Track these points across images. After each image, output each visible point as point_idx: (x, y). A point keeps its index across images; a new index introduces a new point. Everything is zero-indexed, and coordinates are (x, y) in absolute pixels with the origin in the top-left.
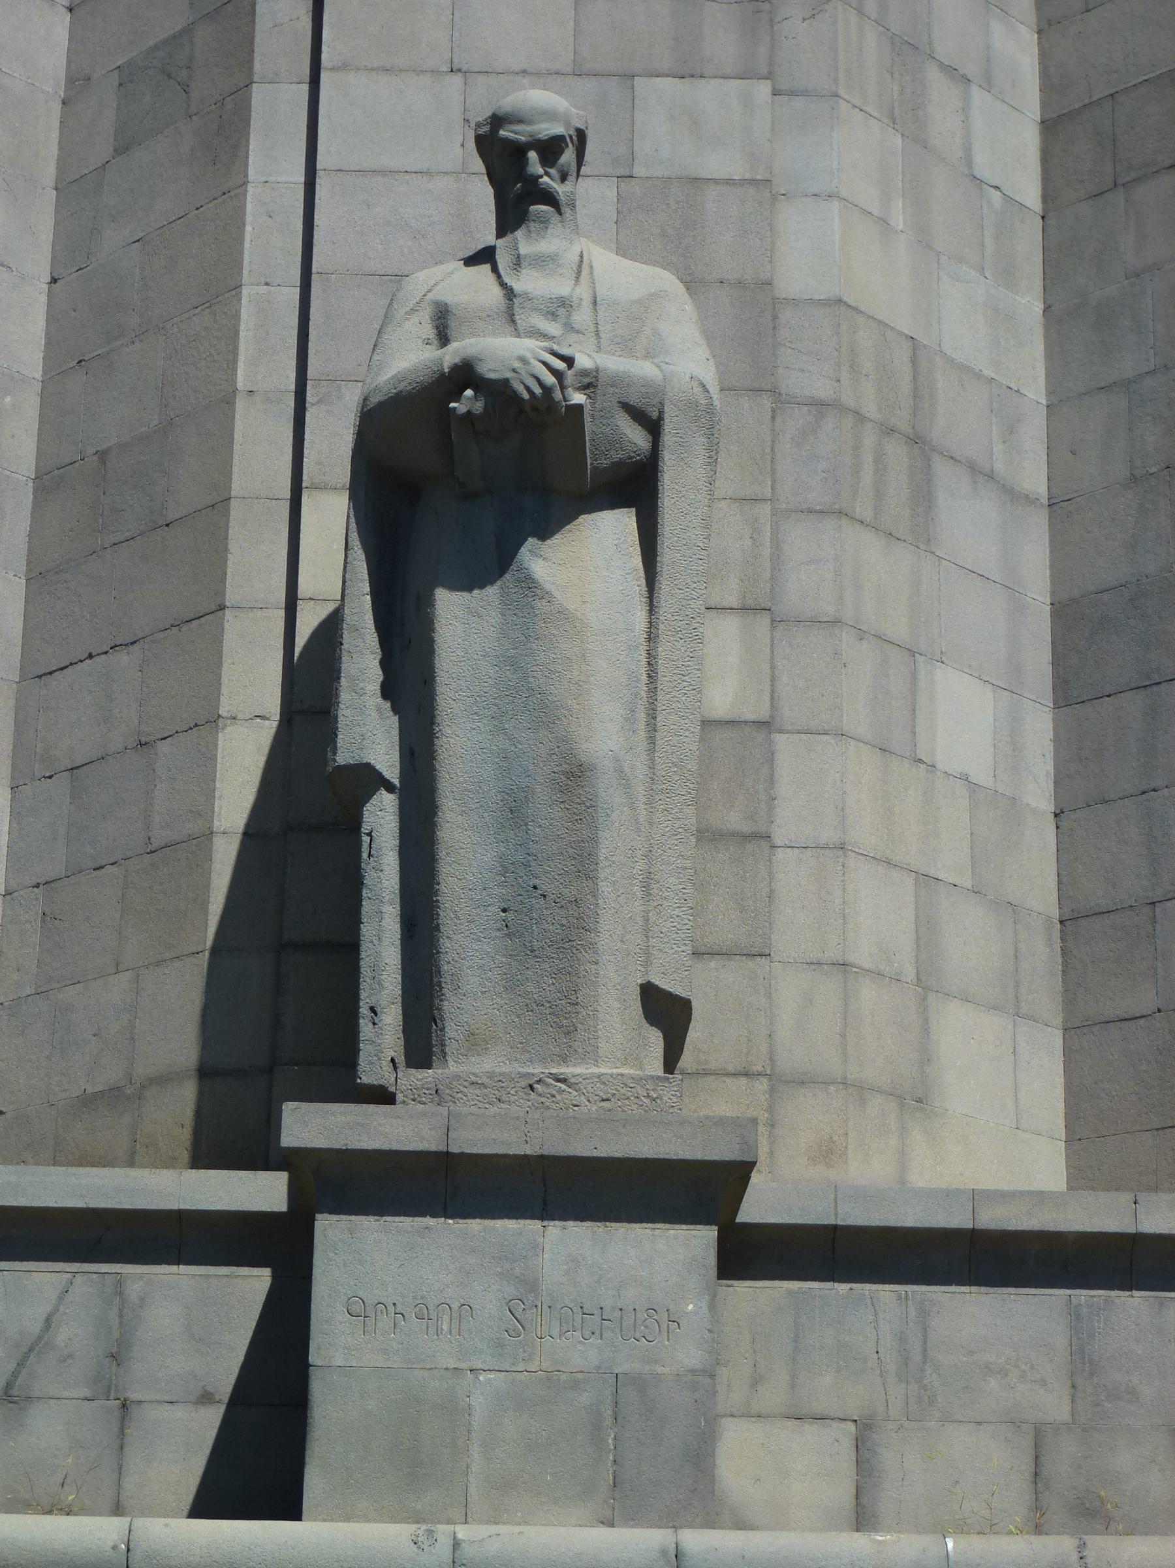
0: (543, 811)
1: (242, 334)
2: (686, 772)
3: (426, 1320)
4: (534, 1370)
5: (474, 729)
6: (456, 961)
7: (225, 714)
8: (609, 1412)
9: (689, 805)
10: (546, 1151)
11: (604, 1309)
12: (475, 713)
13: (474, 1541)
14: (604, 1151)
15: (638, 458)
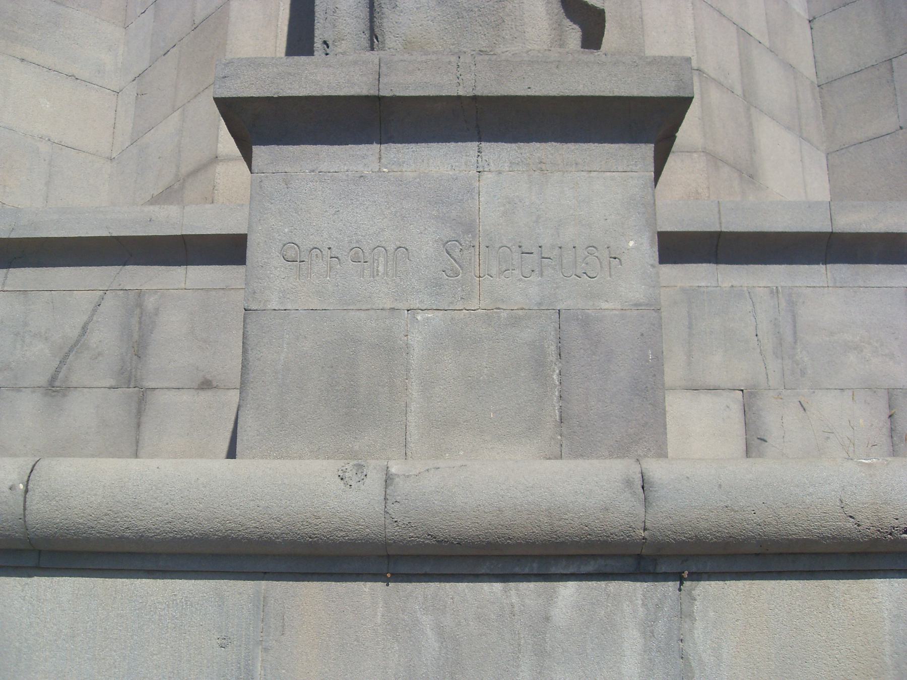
3: (362, 263)
4: (473, 309)
8: (553, 348)
11: (543, 248)
13: (408, 476)
14: (537, 90)
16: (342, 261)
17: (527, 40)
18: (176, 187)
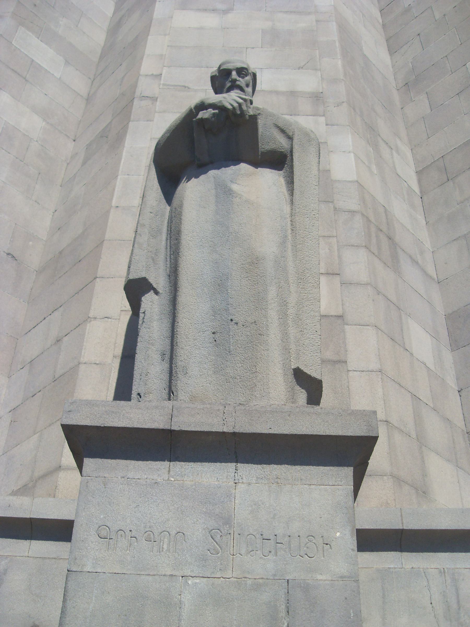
0: (236, 283)
1: (116, 190)
2: (313, 273)
5: (200, 252)
6: (186, 360)
7: (91, 317)
8: (283, 607)
9: (316, 288)
10: (238, 429)
11: (278, 536)
12: (201, 246)
15: (283, 150)
16: (138, 540)
17: (271, 398)
18: (30, 485)
